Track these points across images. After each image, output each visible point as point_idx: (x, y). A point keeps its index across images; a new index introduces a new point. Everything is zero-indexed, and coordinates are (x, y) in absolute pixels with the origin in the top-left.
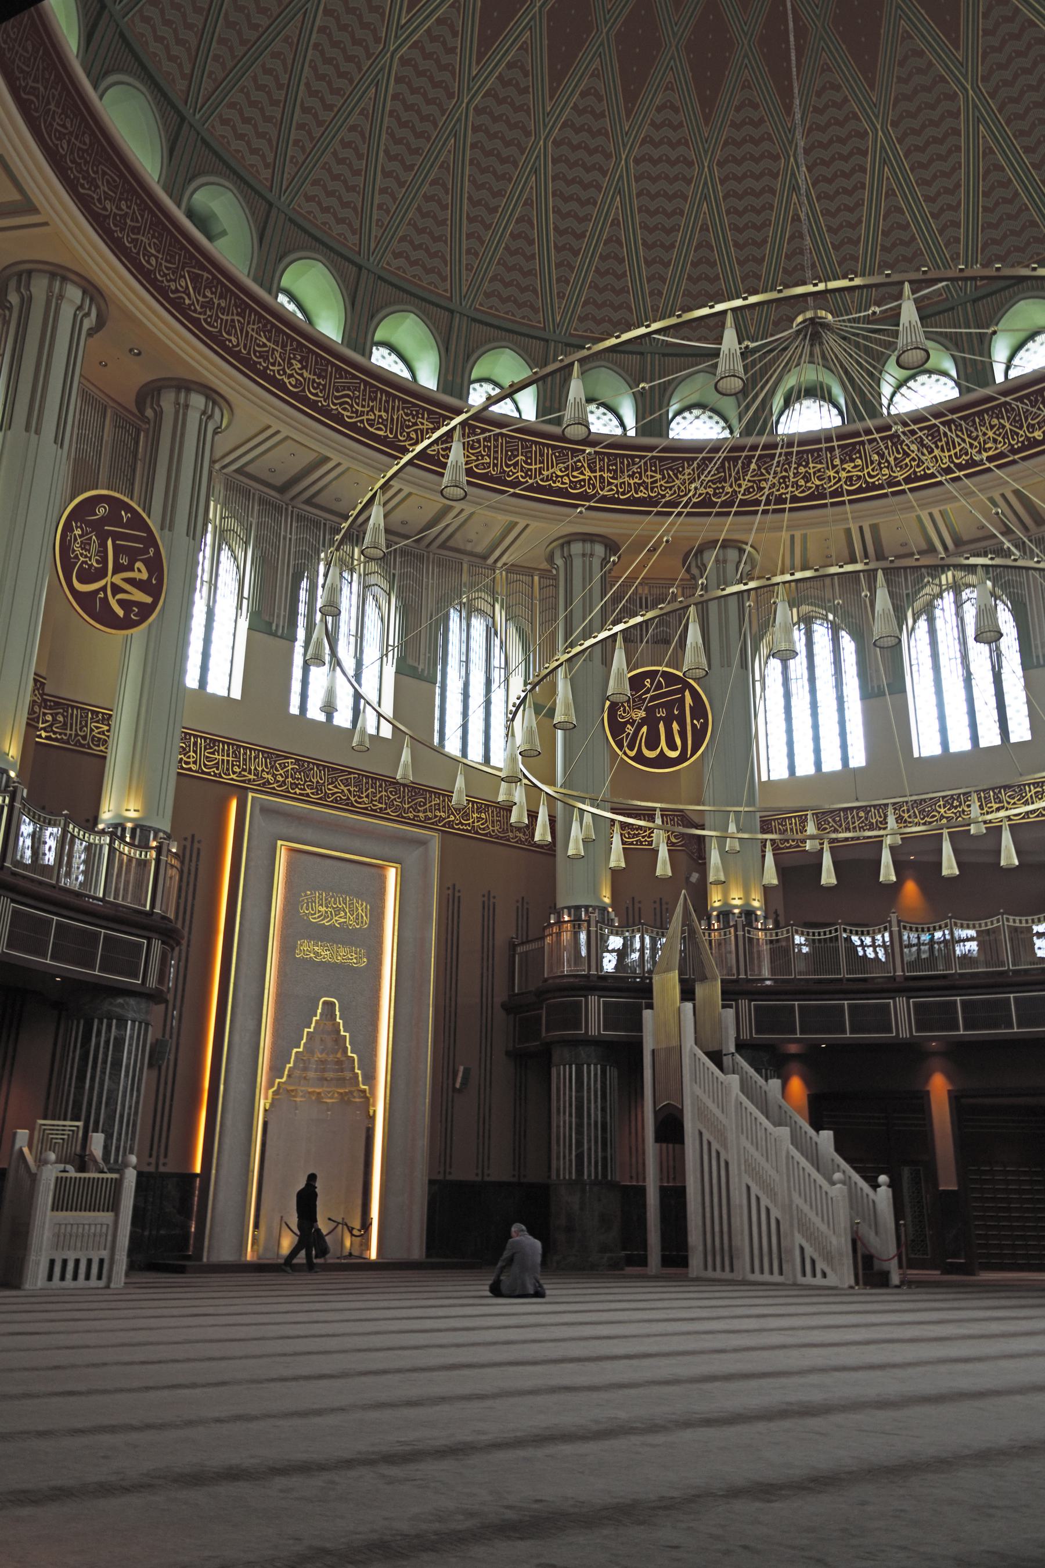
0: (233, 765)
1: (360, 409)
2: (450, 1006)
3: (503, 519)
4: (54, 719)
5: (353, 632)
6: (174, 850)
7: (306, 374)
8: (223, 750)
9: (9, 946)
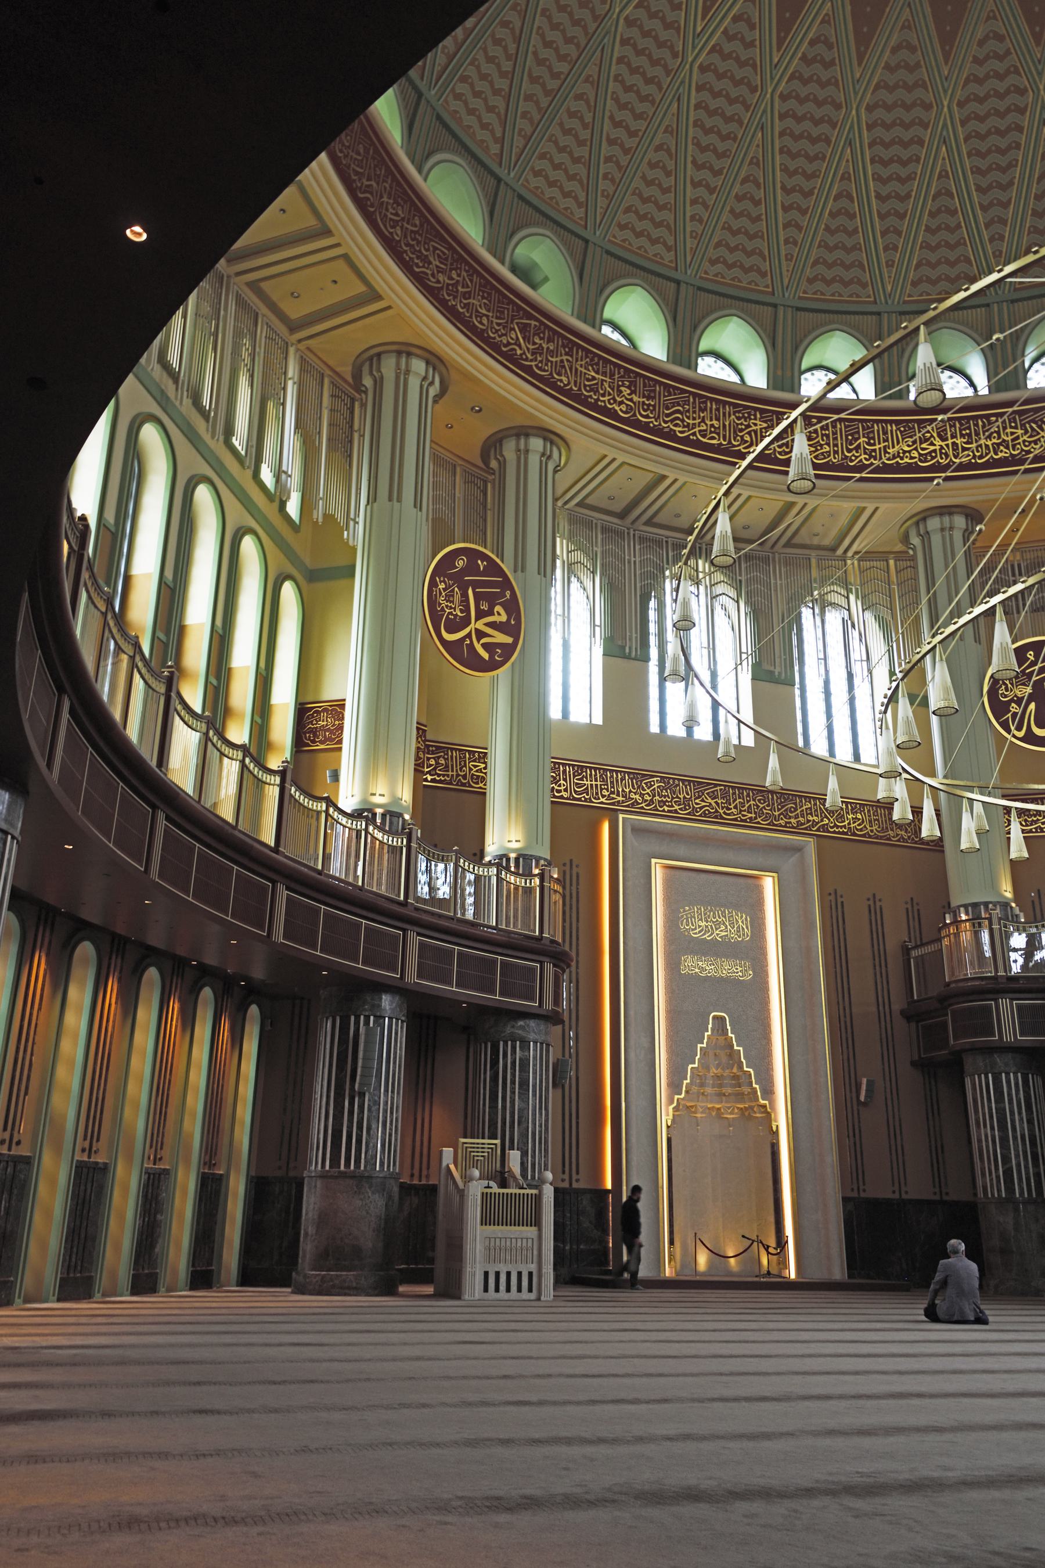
0: (602, 789)
1: (691, 422)
2: (845, 1017)
3: (848, 507)
4: (437, 763)
5: (705, 645)
6: (556, 876)
7: (635, 398)
8: (591, 775)
9: (418, 977)
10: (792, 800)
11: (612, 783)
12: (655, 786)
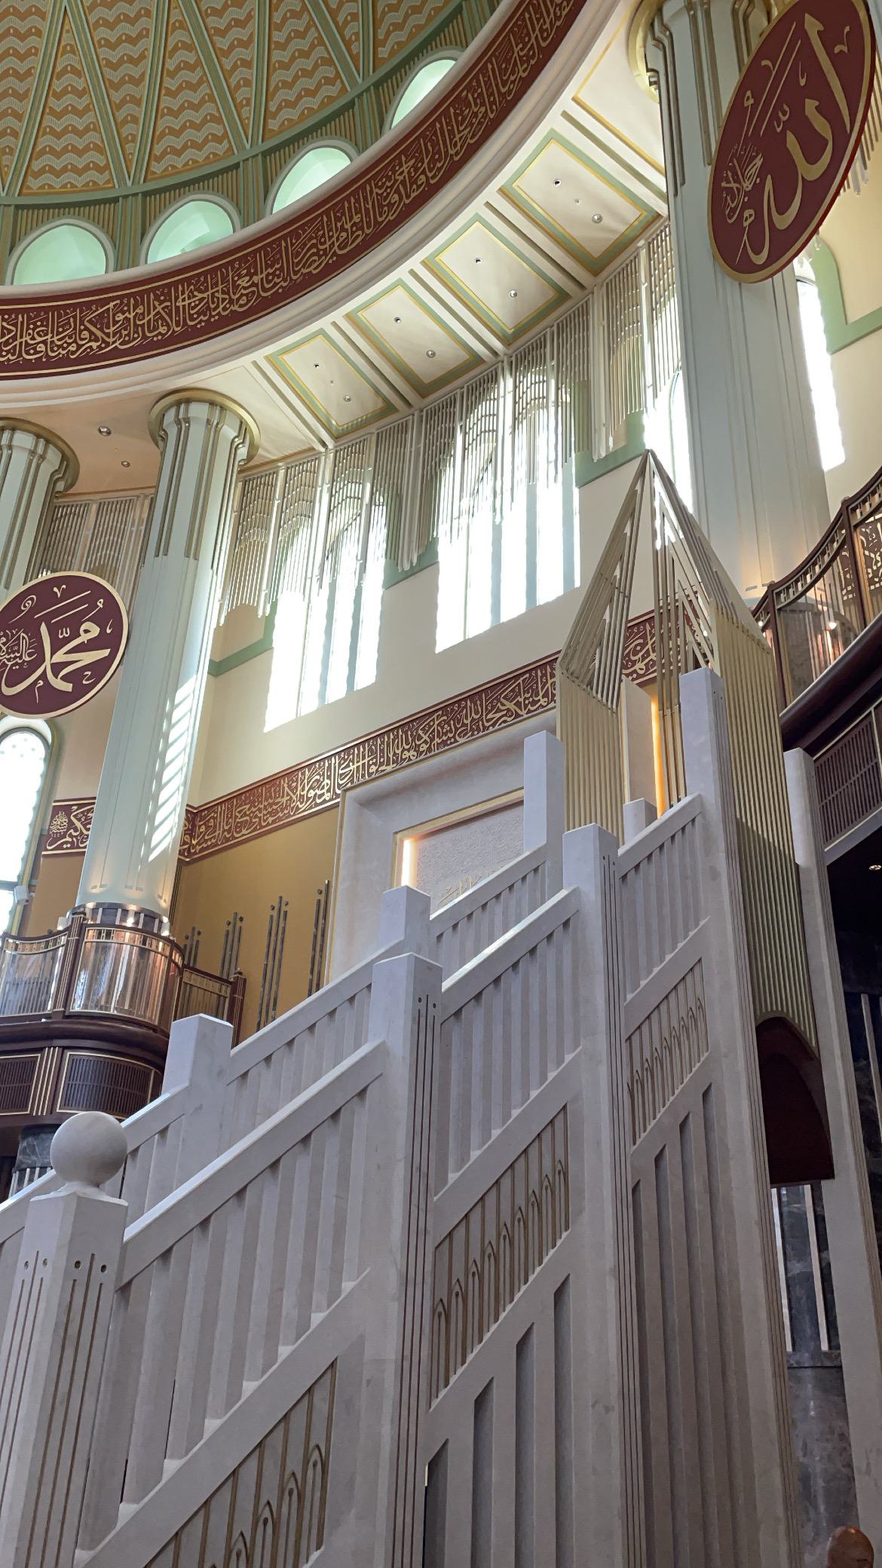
0: (369, 765)
7: (256, 279)
8: (358, 755)
10: (639, 632)
11: (382, 751)
12: (435, 726)
